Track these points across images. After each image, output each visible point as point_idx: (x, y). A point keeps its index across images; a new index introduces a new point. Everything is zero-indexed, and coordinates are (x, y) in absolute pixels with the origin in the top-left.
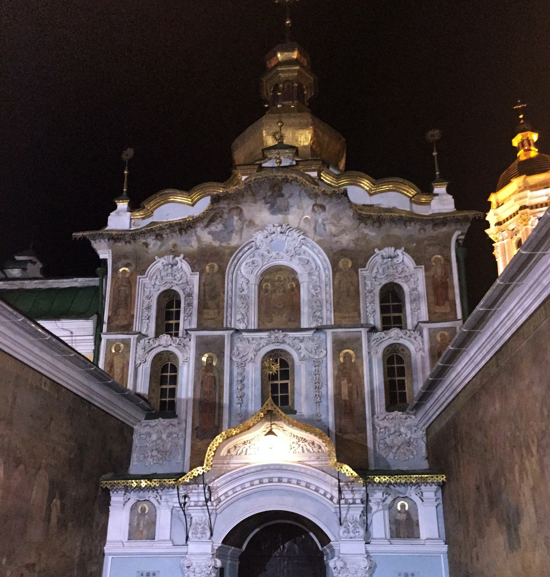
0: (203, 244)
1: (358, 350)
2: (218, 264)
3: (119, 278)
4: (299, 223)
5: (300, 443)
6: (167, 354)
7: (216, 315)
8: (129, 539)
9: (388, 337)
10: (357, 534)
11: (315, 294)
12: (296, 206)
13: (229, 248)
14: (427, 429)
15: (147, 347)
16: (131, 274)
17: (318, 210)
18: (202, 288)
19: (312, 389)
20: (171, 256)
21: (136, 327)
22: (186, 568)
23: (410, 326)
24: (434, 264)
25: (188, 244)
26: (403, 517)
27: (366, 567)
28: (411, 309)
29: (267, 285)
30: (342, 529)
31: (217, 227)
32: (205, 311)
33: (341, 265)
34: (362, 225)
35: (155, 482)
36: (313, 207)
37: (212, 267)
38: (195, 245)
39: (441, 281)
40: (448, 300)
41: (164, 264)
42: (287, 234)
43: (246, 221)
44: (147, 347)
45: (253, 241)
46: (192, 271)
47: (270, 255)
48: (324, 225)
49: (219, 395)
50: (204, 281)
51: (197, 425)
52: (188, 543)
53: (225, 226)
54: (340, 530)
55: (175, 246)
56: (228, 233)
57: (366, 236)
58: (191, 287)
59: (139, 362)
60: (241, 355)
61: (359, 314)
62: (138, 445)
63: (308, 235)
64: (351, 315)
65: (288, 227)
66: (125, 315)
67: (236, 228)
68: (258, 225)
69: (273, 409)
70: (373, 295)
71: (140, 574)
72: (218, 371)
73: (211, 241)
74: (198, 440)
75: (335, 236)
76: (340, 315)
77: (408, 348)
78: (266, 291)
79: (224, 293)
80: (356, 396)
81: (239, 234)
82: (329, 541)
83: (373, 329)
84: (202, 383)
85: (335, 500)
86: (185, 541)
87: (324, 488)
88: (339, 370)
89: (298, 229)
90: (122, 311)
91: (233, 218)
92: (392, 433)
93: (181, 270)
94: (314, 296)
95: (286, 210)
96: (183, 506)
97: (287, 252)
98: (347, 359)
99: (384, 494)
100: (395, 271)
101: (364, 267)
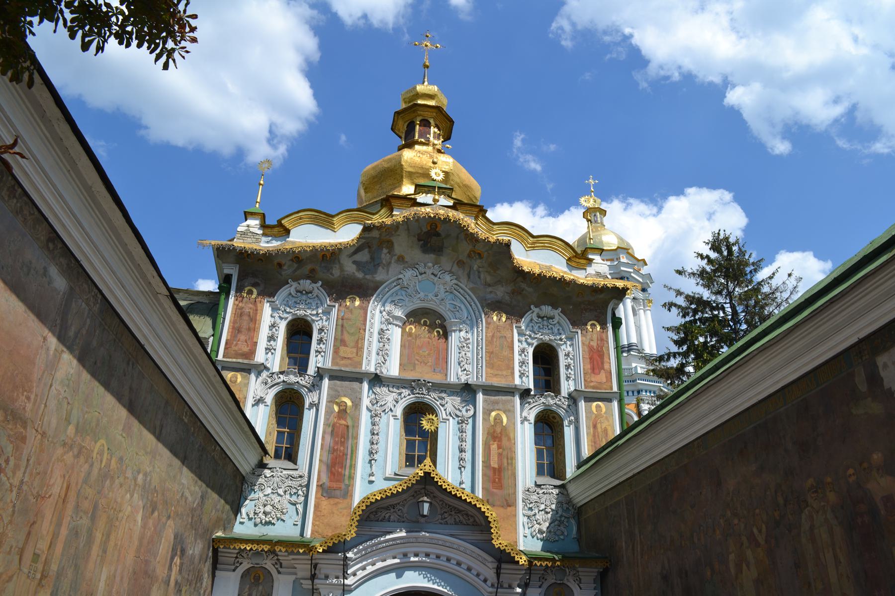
1: (510, 412)
5: (453, 513)
7: (354, 355)
18: (340, 322)
20: (308, 281)
21: (260, 357)
23: (564, 392)
29: (411, 329)
31: (364, 256)
32: (342, 349)
38: (336, 272)
40: (603, 369)
44: (269, 380)
47: (419, 296)
51: (325, 479)
53: (372, 258)
55: (313, 271)
59: (258, 397)
61: (513, 373)
64: (504, 373)
67: (384, 262)
75: (489, 285)
78: (410, 334)
83: (525, 394)
85: (489, 583)
87: (477, 566)
88: (488, 434)
89: (450, 272)
90: (242, 337)
96: (313, 577)
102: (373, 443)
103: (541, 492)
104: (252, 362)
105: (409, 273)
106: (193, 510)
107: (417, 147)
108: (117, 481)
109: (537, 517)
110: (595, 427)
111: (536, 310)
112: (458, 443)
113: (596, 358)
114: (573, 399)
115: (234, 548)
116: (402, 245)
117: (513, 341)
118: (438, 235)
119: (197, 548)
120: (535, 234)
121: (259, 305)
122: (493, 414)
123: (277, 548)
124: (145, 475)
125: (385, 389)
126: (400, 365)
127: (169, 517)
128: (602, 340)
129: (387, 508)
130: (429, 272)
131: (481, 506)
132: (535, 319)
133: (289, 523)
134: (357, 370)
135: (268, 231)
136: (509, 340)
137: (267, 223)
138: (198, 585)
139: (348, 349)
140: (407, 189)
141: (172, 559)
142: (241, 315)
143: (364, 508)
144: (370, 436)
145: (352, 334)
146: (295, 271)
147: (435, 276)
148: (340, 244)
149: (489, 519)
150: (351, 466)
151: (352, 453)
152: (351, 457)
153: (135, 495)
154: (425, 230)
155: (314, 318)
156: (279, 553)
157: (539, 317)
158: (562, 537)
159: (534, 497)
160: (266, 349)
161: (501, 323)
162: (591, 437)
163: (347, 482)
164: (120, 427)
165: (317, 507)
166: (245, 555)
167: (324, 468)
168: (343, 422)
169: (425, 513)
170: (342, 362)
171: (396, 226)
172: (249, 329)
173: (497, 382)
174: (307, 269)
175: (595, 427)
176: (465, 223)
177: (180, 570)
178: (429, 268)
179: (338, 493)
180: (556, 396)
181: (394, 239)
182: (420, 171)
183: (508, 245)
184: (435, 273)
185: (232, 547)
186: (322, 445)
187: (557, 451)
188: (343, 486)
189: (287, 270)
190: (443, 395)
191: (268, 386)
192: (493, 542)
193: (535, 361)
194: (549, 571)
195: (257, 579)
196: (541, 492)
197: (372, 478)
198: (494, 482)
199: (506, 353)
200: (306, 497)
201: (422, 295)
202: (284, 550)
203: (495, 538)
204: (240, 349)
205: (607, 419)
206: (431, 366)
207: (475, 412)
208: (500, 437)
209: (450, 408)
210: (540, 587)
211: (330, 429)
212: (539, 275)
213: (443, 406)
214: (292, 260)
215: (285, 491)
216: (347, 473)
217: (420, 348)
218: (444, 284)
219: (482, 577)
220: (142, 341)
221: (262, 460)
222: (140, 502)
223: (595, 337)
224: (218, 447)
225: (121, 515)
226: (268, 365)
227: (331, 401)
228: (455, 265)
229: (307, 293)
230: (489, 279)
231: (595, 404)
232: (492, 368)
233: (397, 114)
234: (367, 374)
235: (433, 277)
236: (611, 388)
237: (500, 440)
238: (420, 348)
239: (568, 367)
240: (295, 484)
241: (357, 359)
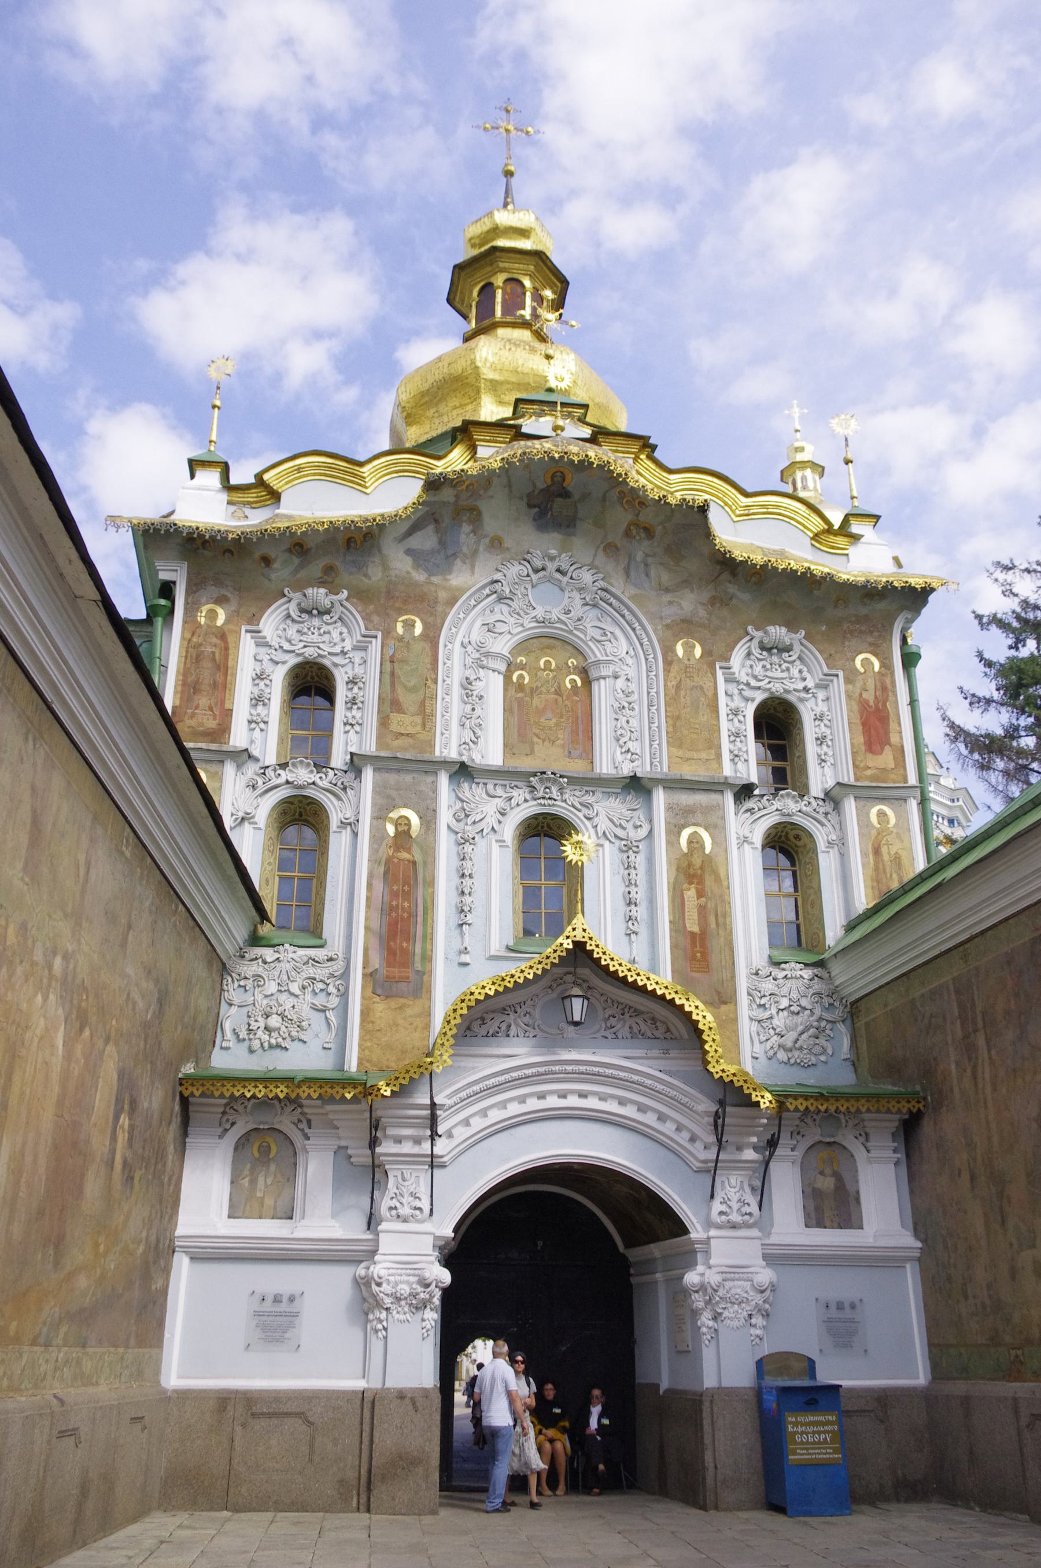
0: (393, 573)
1: (717, 829)
2: (422, 620)
3: (200, 626)
4: (595, 555)
6: (300, 802)
7: (419, 728)
8: (229, 1217)
9: (774, 808)
10: (747, 1217)
11: (626, 705)
12: (591, 521)
13: (444, 588)
14: (853, 1004)
15: (260, 782)
16: (228, 621)
17: (638, 533)
18: (388, 667)
19: (621, 903)
21: (239, 737)
22: (374, 1286)
24: (862, 670)
25: (360, 569)
26: (827, 1183)
27: (762, 1292)
28: (819, 756)
29: (521, 677)
30: (717, 1206)
31: (426, 540)
32: (395, 717)
33: (680, 651)
34: (726, 576)
35: (310, 1087)
36: (629, 525)
37: (410, 625)
39: (876, 705)
40: (890, 745)
41: (303, 604)
42: (569, 575)
43: (486, 536)
44: (260, 782)
45: (497, 581)
46: (366, 629)
47: (534, 613)
48: (646, 565)
49: (425, 902)
50: (391, 653)
51: (376, 963)
52: (380, 1228)
53: (442, 543)
54: (710, 1209)
55: (329, 569)
56: (447, 557)
57: (731, 598)
58: (361, 662)
59: (241, 814)
60: (470, 821)
61: (719, 756)
62: (236, 1001)
63: (613, 581)
65: (573, 560)
66: (212, 710)
67: (465, 549)
68: (508, 549)
69: (586, 939)
70: (742, 718)
71: (257, 1298)
72: (422, 850)
73: (409, 569)
74: (378, 999)
75: (667, 590)
76: (680, 753)
77: (811, 836)
78: (520, 687)
79: (436, 682)
80: (713, 925)
81: (467, 561)
82: (683, 1230)
83: (744, 792)
84: (386, 873)
85: (699, 1145)
86: (365, 1226)
88: (677, 870)
89: (592, 566)
90: (203, 701)
91: (461, 526)
92: (782, 1007)
93: (339, 624)
94: (624, 707)
95: (568, 526)
96: (373, 1143)
97: (567, 612)
98: (696, 845)
99: (795, 1134)
100: (785, 675)
101: (728, 660)
102: (463, 892)
103: (781, 975)
104: (225, 748)
105: (515, 570)
106: (146, 1025)
107: (501, 332)
108: (19, 970)
109: (776, 1022)
110: (877, 852)
111: (758, 634)
112: (622, 889)
113: (874, 724)
114: (833, 798)
115: (222, 1096)
116: (497, 515)
117: (716, 695)
118: (565, 494)
119: (156, 1099)
120: (749, 490)
121: (231, 639)
122: (686, 833)
123: (304, 1092)
124: (66, 957)
125: (479, 791)
126: (505, 745)
127: (107, 1040)
128: (884, 689)
129: (503, 1010)
130: (551, 566)
131: (683, 1001)
132: (756, 651)
133: (315, 1046)
134: (427, 757)
135: (237, 497)
136: (710, 694)
137: (234, 480)
138: (159, 1166)
139: (407, 719)
140: (491, 410)
141: (117, 1118)
142: (198, 659)
143: (465, 1011)
144: (457, 881)
145: (413, 690)
146: (296, 571)
147: (563, 573)
148: (382, 515)
149: (700, 1026)
150: (424, 937)
151: (425, 913)
152: (425, 920)
153: (52, 997)
154: (541, 485)
155: (337, 660)
156: (304, 1102)
157: (763, 647)
158: (823, 1058)
159: (768, 986)
160: (250, 722)
161: (692, 661)
162: (870, 871)
163: (418, 966)
164: (19, 865)
165: (365, 1014)
166: (240, 1108)
167: (374, 942)
168: (404, 855)
169: (577, 1018)
170: (396, 743)
171: (487, 479)
172: (215, 685)
173: (689, 772)
174: (316, 569)
175: (877, 852)
176: (619, 470)
177: (131, 1139)
178: (552, 559)
179: (403, 986)
180: (802, 796)
181: (482, 505)
182: (513, 379)
183: (703, 509)
184: (564, 567)
185: (217, 1094)
186: (368, 899)
187: (803, 901)
188: (412, 975)
189: (280, 571)
190: (589, 799)
191: (258, 792)
192: (710, 1067)
193: (758, 736)
194: (809, 1121)
195: (265, 1151)
196: (784, 973)
197: (466, 958)
198: (694, 958)
199: (704, 717)
200: (344, 995)
201: (539, 612)
202: (315, 1096)
203: (713, 1062)
204: (201, 724)
205: (899, 836)
206: (563, 746)
207: (651, 832)
208: (697, 874)
209: (603, 824)
210: (793, 1150)
211: (382, 869)
212: (764, 566)
213: (589, 819)
214: (290, 551)
215: (304, 988)
216: (418, 949)
217: (541, 712)
218: (581, 590)
219: (686, 1135)
220: (49, 696)
221: (255, 930)
222: (60, 1011)
223: (871, 684)
224: (181, 907)
225: (28, 1035)
226: (255, 752)
227: (380, 816)
228: (601, 552)
229: (321, 613)
230: (665, 578)
231: (874, 811)
232: (680, 747)
233: (459, 269)
234: (445, 763)
235: (558, 576)
236: (906, 781)
237: (701, 881)
238: (541, 712)
239: (821, 740)
240: (321, 973)
241: (422, 737)
